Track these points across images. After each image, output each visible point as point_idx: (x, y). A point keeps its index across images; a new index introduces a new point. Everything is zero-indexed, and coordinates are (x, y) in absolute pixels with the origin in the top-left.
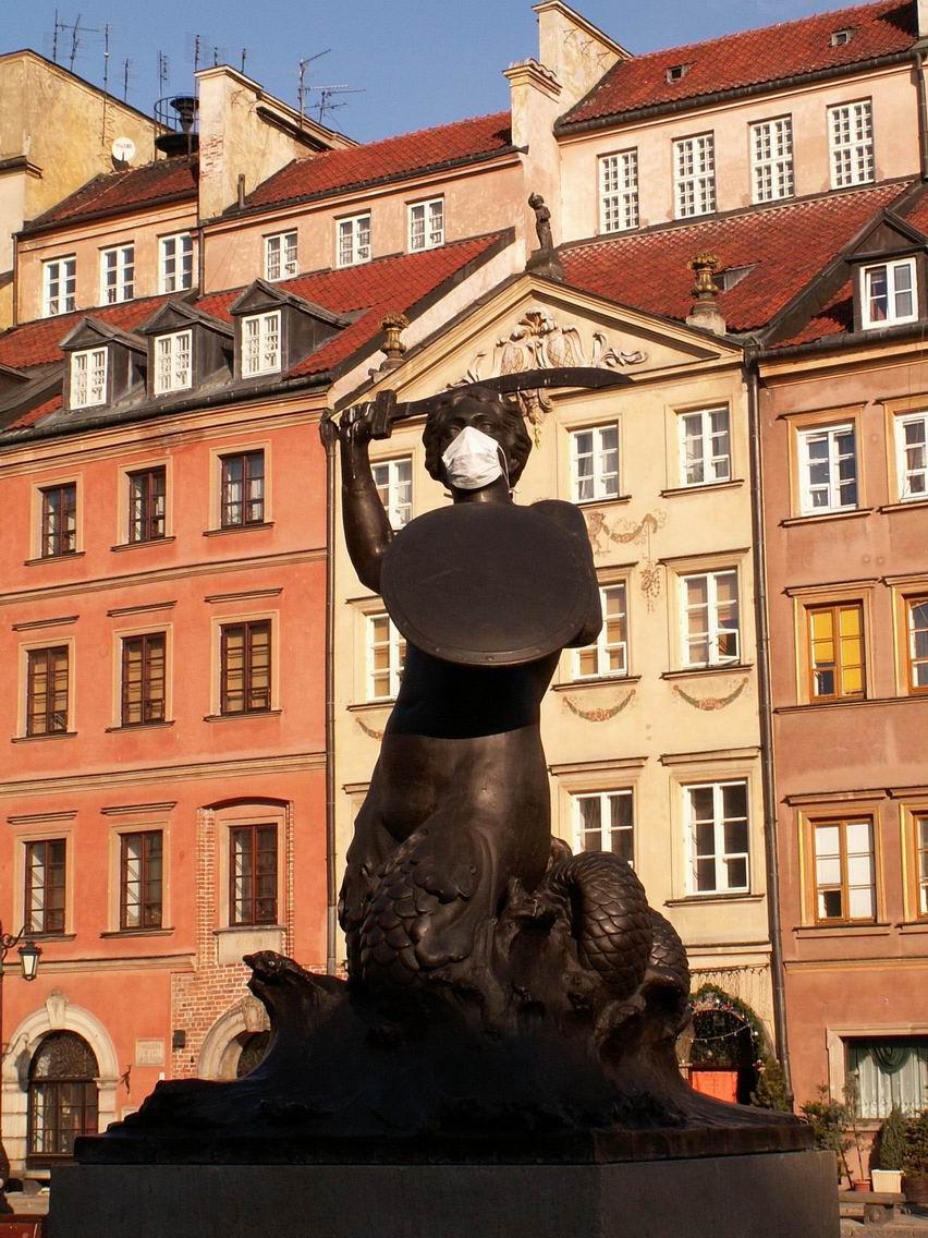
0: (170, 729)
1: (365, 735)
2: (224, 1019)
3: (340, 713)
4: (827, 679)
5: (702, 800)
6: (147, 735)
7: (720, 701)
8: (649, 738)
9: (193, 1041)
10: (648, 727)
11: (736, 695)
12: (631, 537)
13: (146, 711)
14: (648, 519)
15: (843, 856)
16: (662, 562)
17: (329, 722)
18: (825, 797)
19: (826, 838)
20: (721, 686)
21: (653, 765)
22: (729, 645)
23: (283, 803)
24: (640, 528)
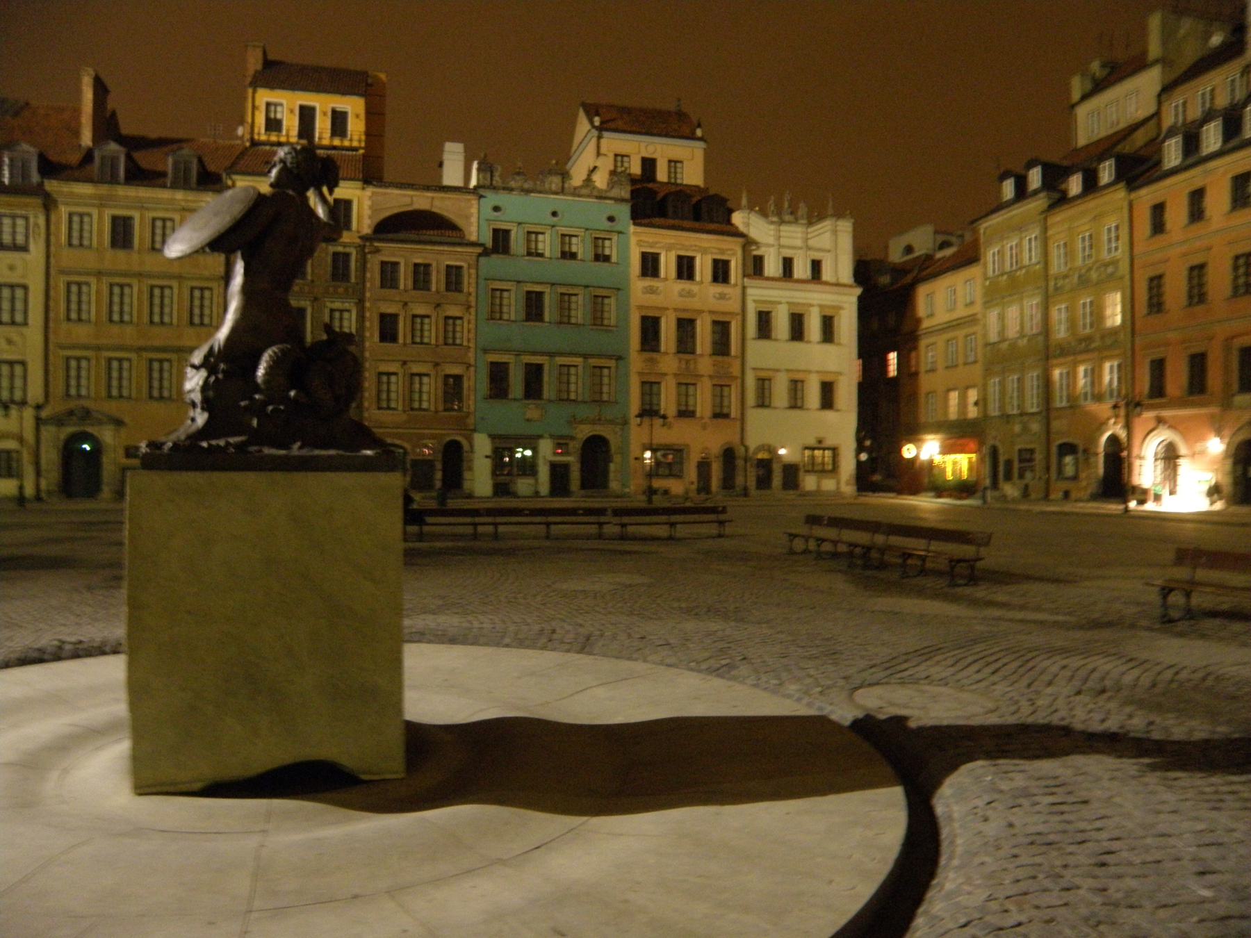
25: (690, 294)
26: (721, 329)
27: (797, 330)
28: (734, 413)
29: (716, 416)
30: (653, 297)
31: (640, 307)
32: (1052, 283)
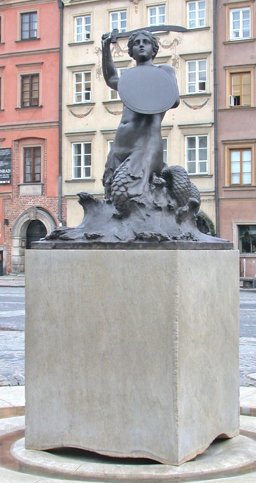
0: (2, 113)
2: (22, 216)
3: (64, 107)
4: (237, 100)
5: (191, 141)
7: (199, 106)
8: (174, 119)
9: (12, 223)
10: (173, 115)
11: (205, 104)
12: (169, 47)
14: (175, 40)
15: (241, 162)
16: (181, 56)
17: (60, 110)
18: (236, 142)
19: (235, 156)
20: (200, 102)
21: (176, 128)
22: (202, 86)
23: (44, 139)
24: (172, 43)
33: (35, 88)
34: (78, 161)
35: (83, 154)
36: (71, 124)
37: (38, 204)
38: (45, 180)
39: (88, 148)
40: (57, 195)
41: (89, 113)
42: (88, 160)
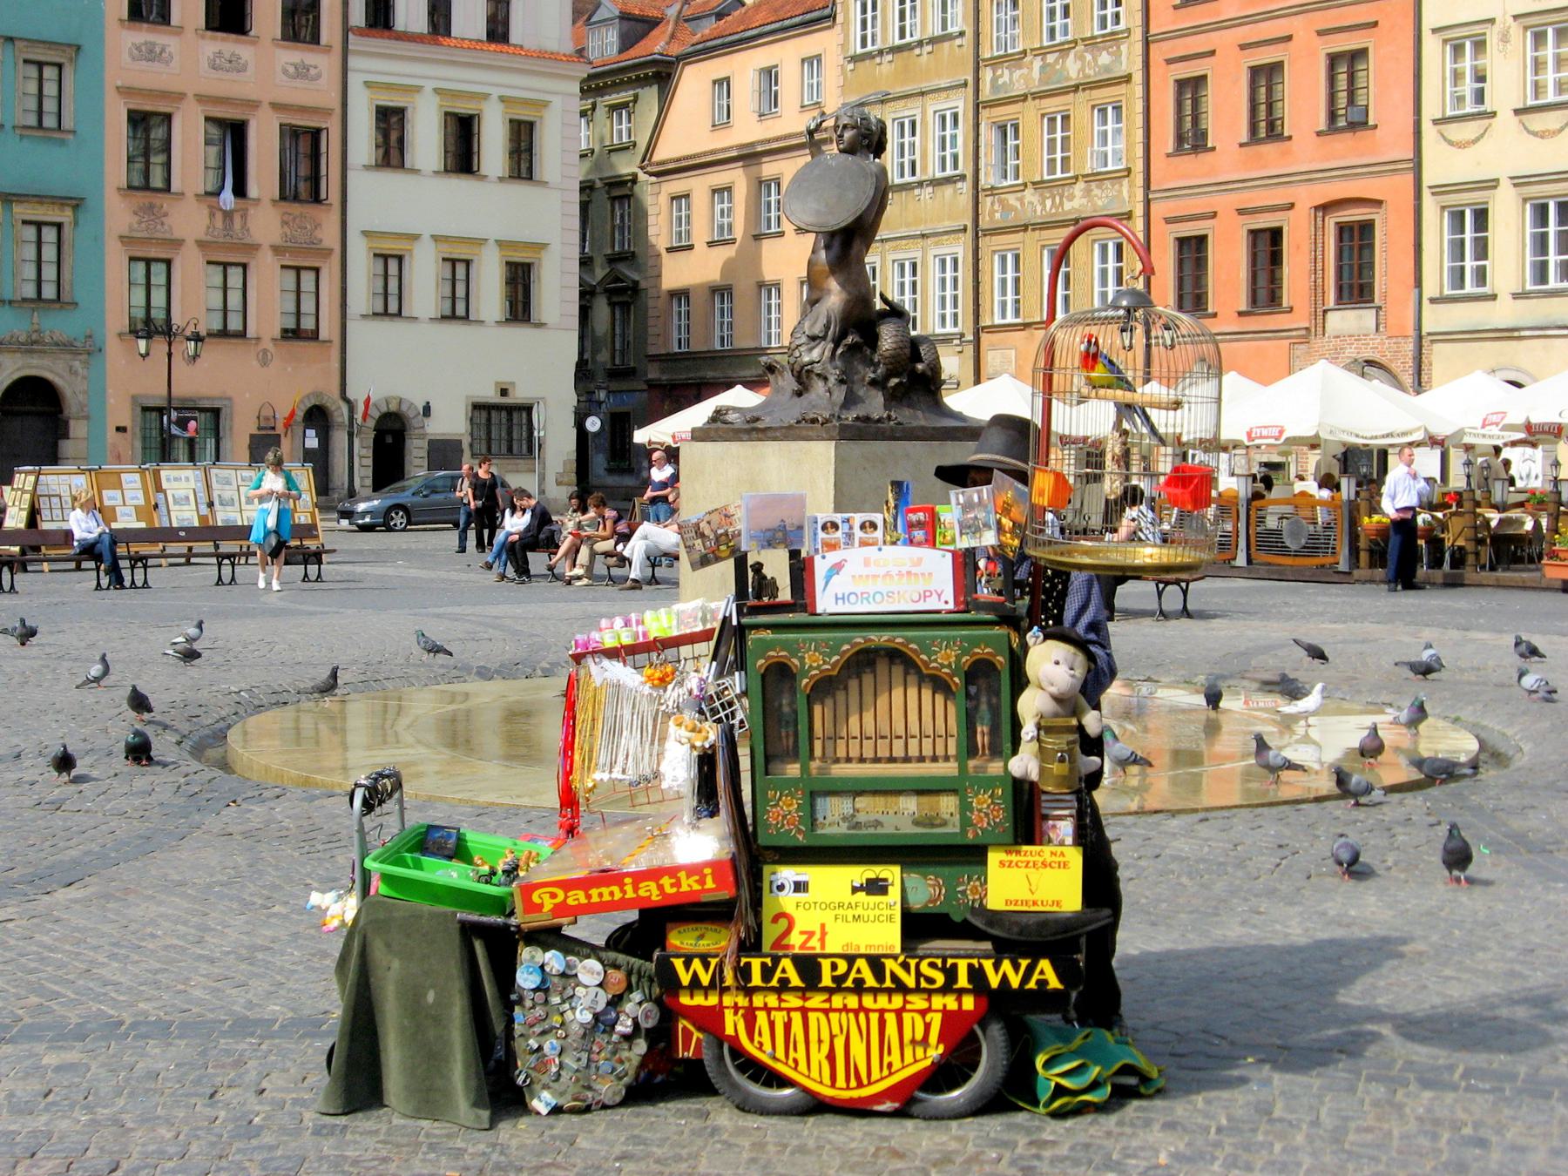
1: (1445, 144)
6: (1269, 149)
13: (1266, 126)
25: (236, 65)
26: (306, 147)
27: (462, 151)
28: (328, 330)
29: (293, 334)
30: (156, 66)
31: (125, 91)
32: (987, 75)
33: (1360, 83)
34: (1458, 249)
35: (1469, 235)
36: (1444, 163)
37: (1369, 355)
38: (1385, 297)
39: (1481, 217)
40: (1411, 332)
41: (1482, 136)
42: (1482, 250)
